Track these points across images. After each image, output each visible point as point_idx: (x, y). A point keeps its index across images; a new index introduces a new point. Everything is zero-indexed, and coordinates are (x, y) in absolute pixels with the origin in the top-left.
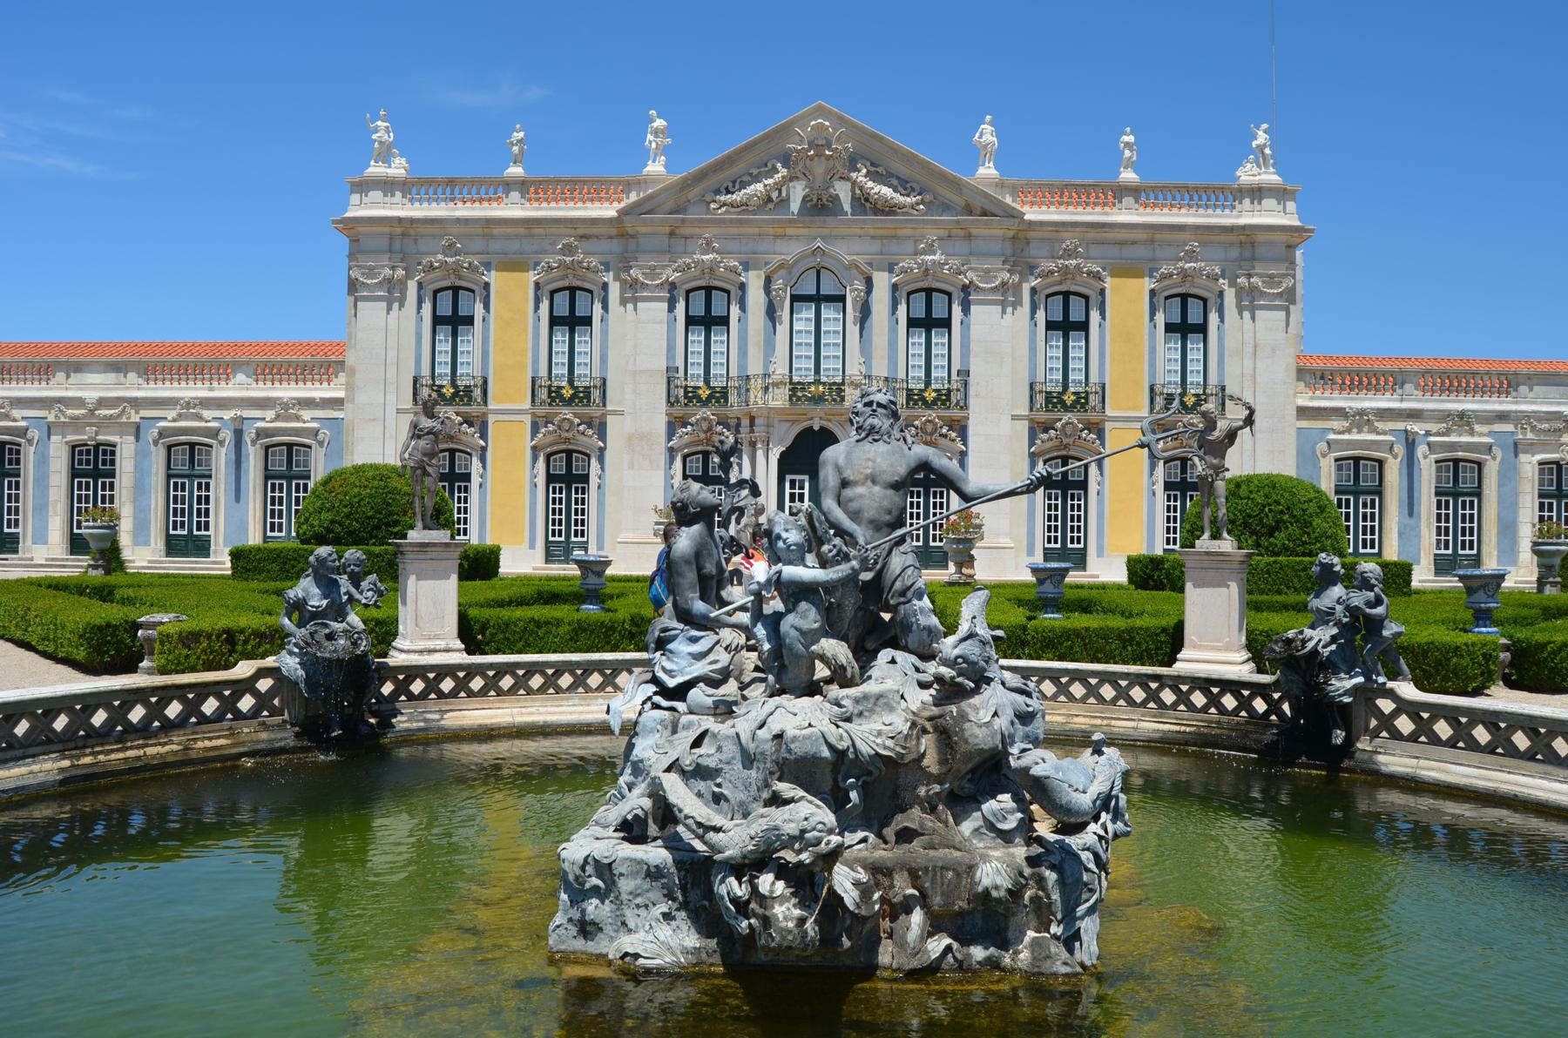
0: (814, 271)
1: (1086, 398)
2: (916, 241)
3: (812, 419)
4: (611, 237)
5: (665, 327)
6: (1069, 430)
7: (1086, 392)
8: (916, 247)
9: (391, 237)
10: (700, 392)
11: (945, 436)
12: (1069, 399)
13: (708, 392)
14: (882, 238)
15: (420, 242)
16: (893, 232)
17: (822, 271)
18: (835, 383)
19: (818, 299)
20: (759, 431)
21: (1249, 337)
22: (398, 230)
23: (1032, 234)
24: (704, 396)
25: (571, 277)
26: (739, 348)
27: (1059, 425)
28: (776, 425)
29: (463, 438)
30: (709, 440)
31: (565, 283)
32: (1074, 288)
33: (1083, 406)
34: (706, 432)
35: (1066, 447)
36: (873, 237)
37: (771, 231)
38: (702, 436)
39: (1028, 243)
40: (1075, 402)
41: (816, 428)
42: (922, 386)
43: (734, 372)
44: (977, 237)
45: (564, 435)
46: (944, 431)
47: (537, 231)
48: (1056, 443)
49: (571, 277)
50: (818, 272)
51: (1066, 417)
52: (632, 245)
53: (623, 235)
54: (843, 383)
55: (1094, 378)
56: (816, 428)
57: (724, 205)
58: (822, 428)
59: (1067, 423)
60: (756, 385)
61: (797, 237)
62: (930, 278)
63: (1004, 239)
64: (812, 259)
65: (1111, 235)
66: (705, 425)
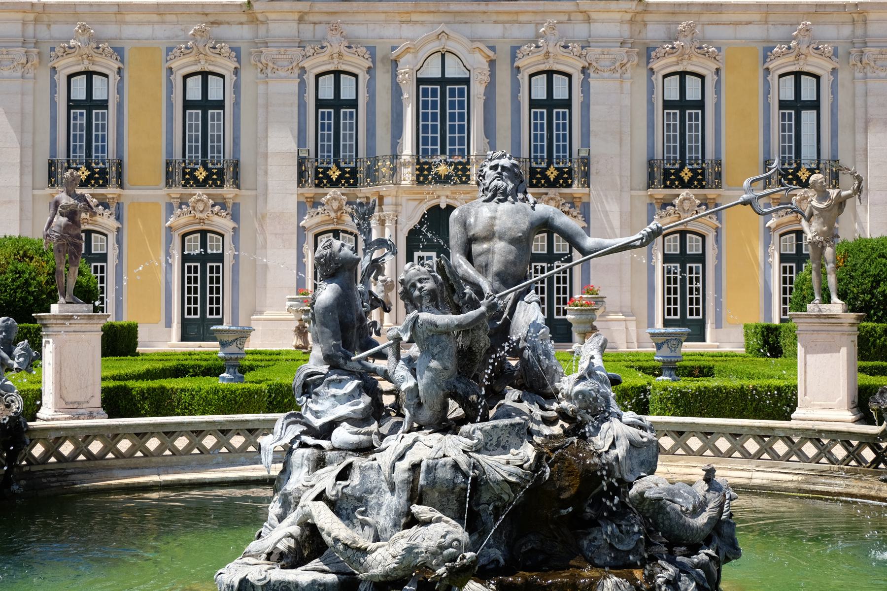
0: (439, 55)
1: (703, 174)
4: (242, 23)
5: (296, 109)
6: (687, 205)
7: (703, 168)
8: (537, 31)
9: (24, 23)
10: (330, 173)
11: (567, 213)
12: (686, 174)
13: (338, 173)
14: (503, 22)
15: (53, 26)
16: (515, 18)
17: (447, 55)
18: (460, 163)
19: (443, 81)
20: (388, 210)
21: (860, 113)
22: (31, 16)
23: (648, 17)
24: (334, 177)
25: (203, 62)
26: (368, 130)
27: (677, 201)
28: (404, 204)
32: (690, 68)
33: (700, 181)
36: (495, 22)
37: (398, 18)
38: (333, 215)
39: (645, 25)
40: (691, 180)
42: (544, 165)
43: (362, 154)
44: (595, 21)
45: (199, 215)
46: (567, 209)
47: (168, 18)
49: (203, 62)
50: (443, 56)
51: (684, 193)
52: (262, 30)
53: (254, 21)
54: (468, 163)
55: (710, 155)
56: (443, 206)
59: (684, 199)
60: (384, 168)
61: (423, 23)
62: (551, 61)
63: (622, 22)
64: (437, 43)
65: (725, 17)
66: (335, 205)
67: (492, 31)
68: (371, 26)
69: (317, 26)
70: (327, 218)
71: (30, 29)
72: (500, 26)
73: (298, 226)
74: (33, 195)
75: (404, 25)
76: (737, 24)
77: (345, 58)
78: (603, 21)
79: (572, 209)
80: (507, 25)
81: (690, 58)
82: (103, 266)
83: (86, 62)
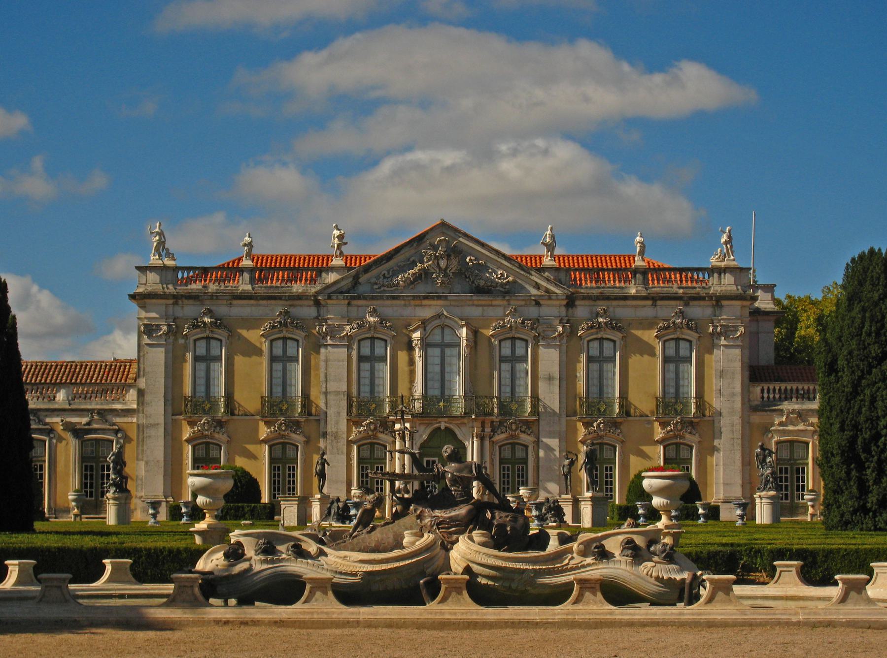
2: (504, 308)
3: (440, 422)
5: (346, 363)
9: (167, 306)
11: (524, 432)
16: (490, 303)
29: (216, 436)
30: (375, 437)
31: (281, 335)
32: (605, 336)
34: (373, 431)
35: (601, 437)
36: (477, 306)
38: (370, 433)
41: (443, 428)
46: (523, 429)
48: (595, 435)
49: (284, 332)
50: (443, 329)
56: (443, 428)
57: (383, 285)
58: (446, 428)
63: (560, 306)
67: (474, 312)
68: (395, 309)
69: (360, 308)
70: (366, 435)
71: (170, 309)
72: (481, 308)
73: (347, 440)
74: (172, 419)
75: (417, 308)
76: (636, 307)
77: (378, 329)
78: (548, 305)
79: (527, 430)
80: (485, 308)
81: (605, 330)
82: (42, 465)
83: (208, 332)
